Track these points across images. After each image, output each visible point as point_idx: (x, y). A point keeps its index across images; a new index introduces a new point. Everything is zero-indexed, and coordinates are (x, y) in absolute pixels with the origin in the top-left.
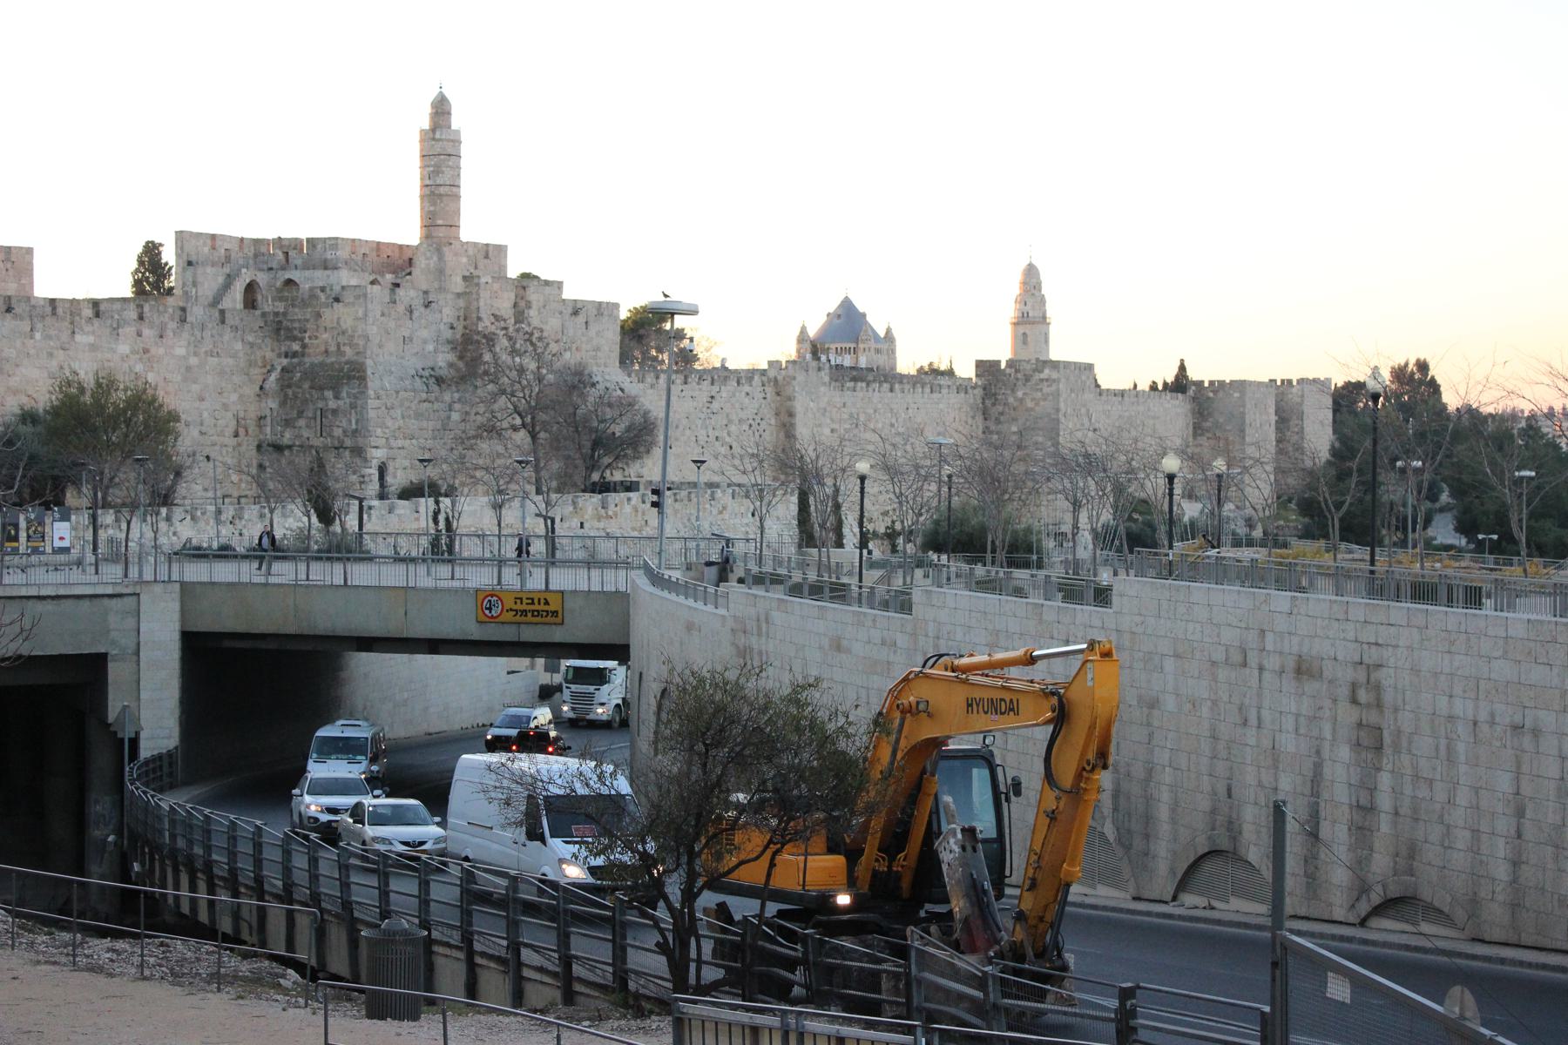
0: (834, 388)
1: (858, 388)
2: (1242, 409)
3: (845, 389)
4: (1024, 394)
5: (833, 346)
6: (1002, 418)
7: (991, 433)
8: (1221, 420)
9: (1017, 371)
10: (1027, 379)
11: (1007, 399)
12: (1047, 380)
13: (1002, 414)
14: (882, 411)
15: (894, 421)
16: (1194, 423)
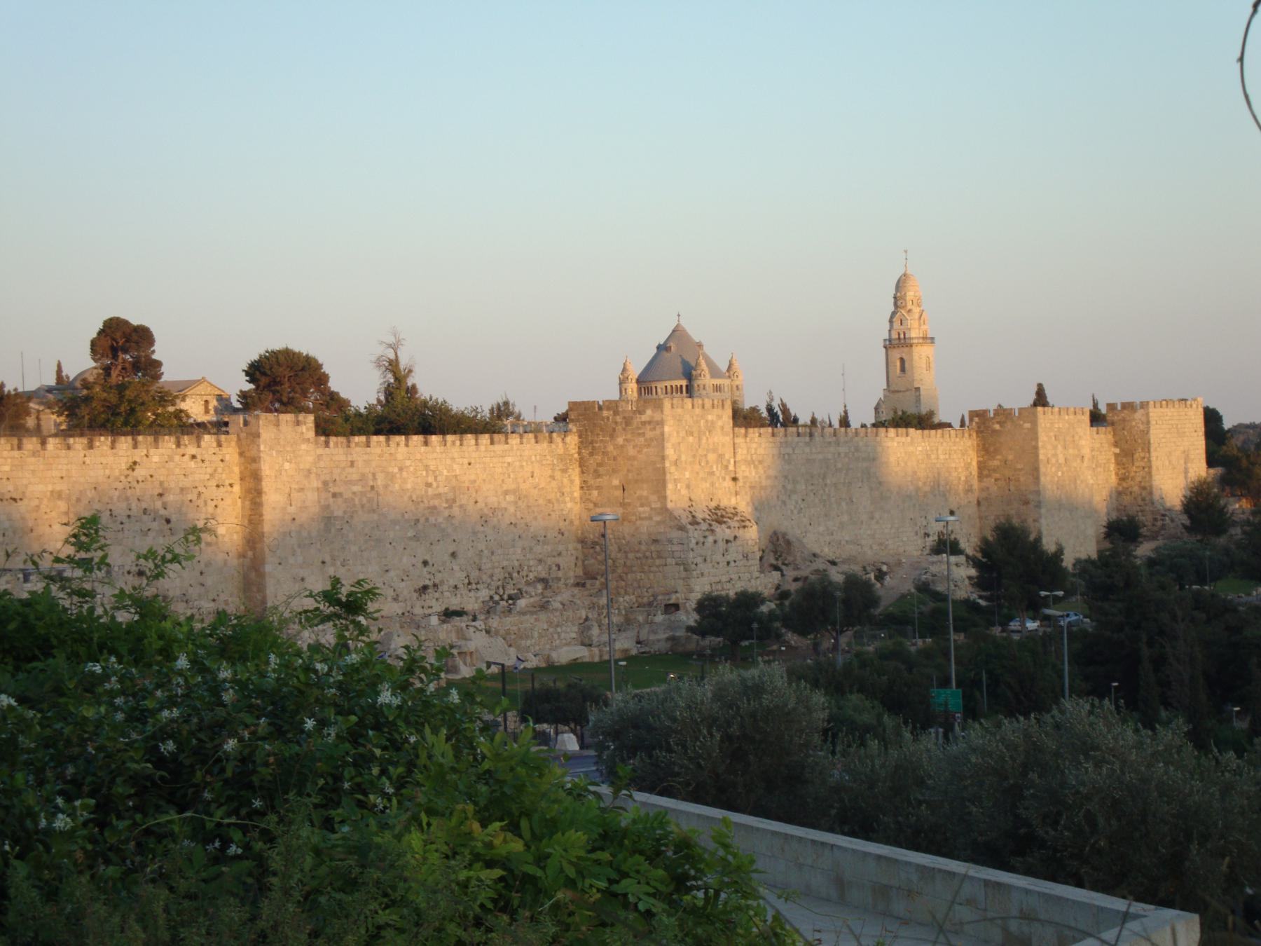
0: (336, 445)
1: (373, 444)
2: (1033, 443)
3: (353, 445)
4: (626, 440)
5: (660, 385)
6: (601, 469)
7: (589, 488)
8: (1010, 457)
9: (616, 413)
10: (628, 421)
11: (605, 447)
12: (649, 423)
13: (599, 465)
14: (412, 469)
15: (431, 479)
16: (979, 463)
